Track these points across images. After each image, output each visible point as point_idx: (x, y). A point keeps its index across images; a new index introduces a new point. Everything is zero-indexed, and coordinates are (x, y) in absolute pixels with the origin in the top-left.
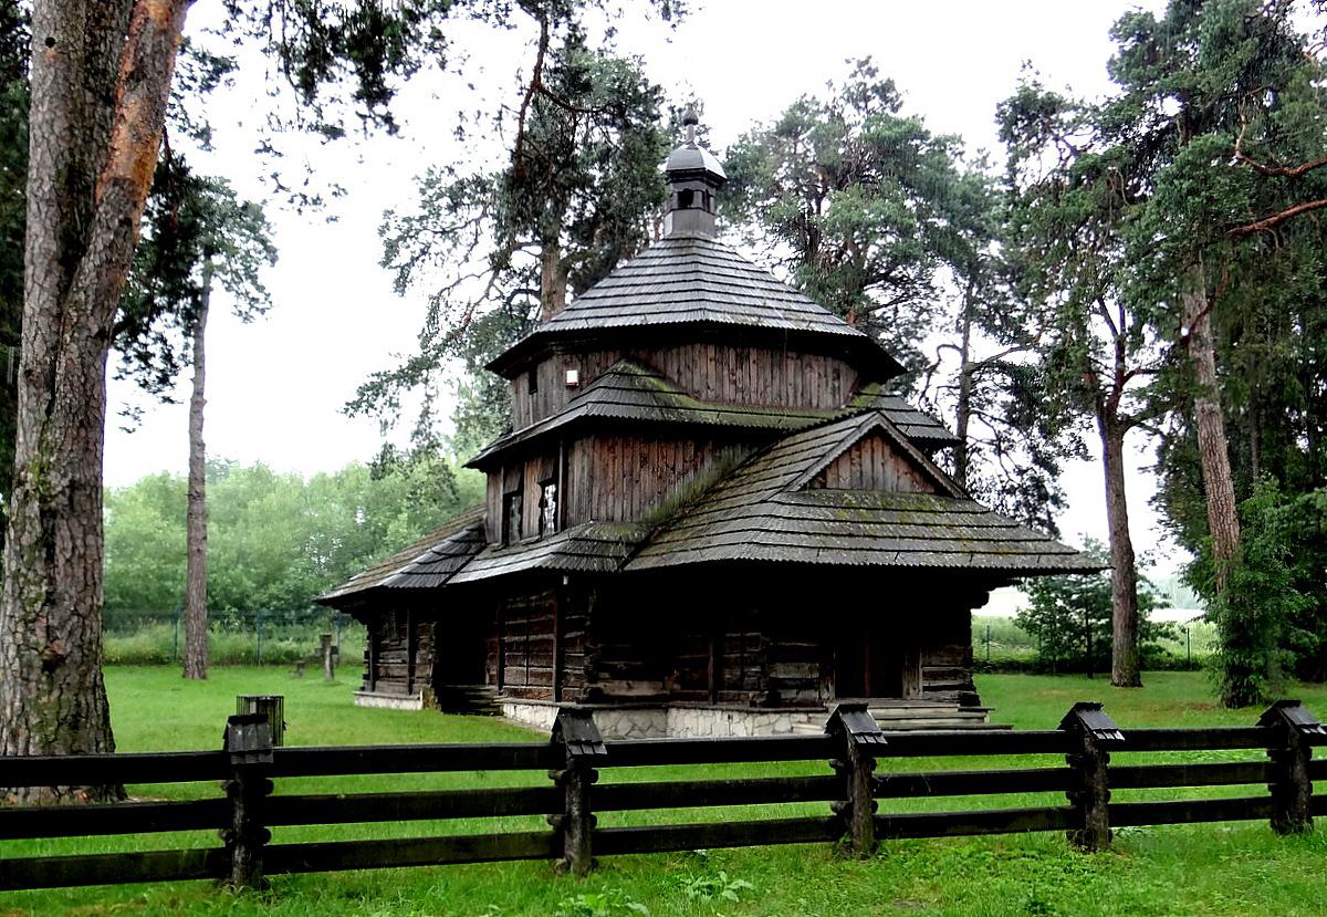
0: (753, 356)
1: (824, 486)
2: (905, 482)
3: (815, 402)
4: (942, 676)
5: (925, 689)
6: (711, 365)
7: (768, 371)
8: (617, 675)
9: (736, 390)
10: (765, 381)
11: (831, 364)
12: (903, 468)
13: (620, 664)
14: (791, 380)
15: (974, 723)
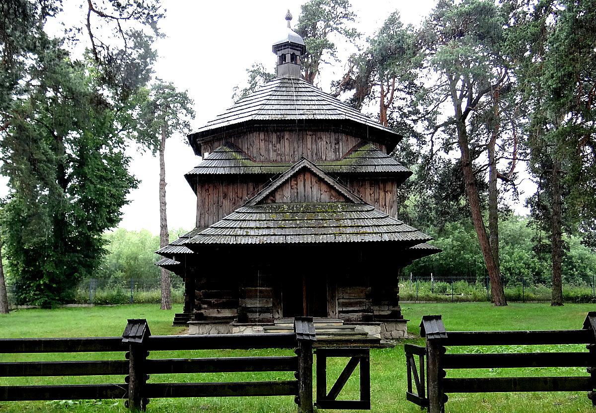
0: (286, 136)
1: (274, 202)
2: (325, 197)
3: (324, 158)
4: (351, 305)
5: (340, 312)
6: (262, 144)
7: (295, 143)
8: (211, 306)
9: (278, 155)
10: (294, 149)
11: (333, 137)
12: (324, 188)
13: (213, 301)
14: (309, 146)
15: (348, 332)
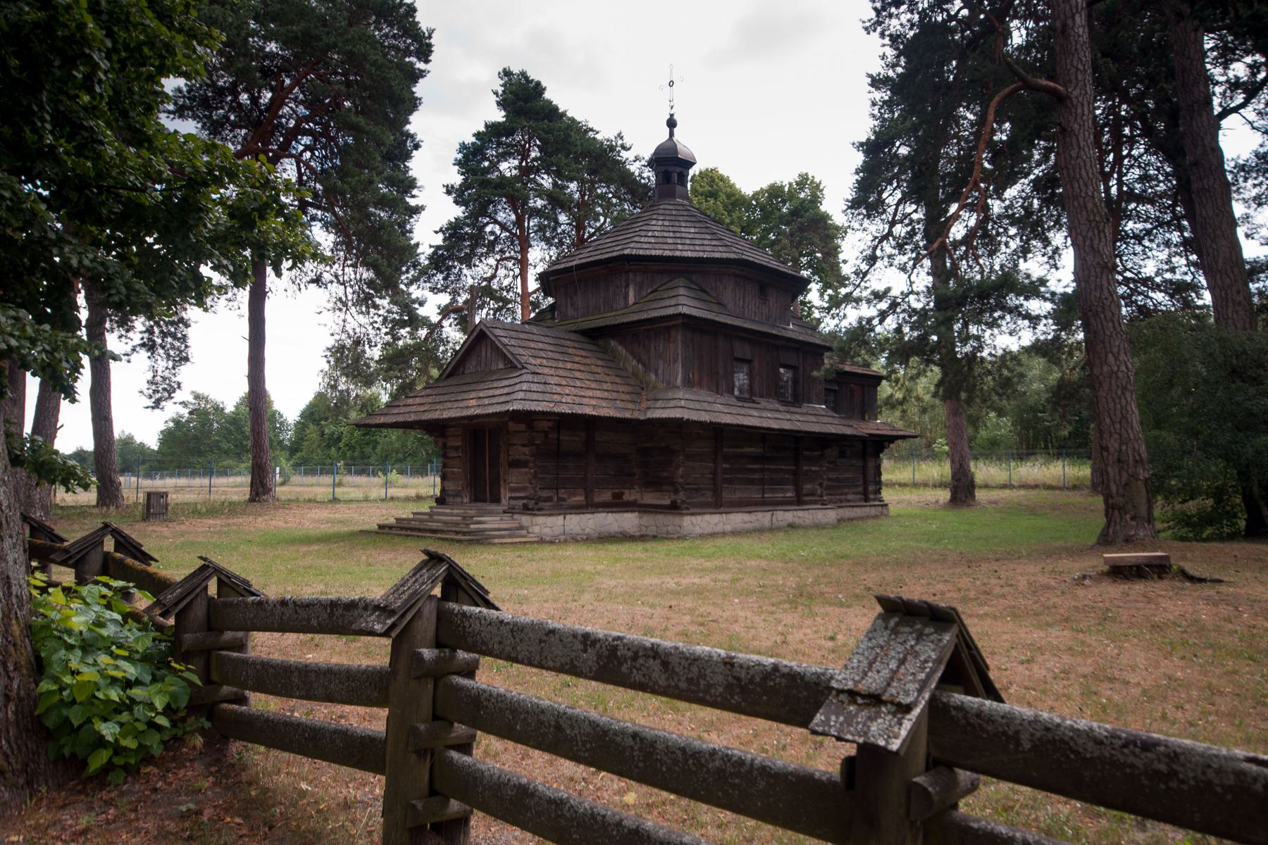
5: (511, 498)
